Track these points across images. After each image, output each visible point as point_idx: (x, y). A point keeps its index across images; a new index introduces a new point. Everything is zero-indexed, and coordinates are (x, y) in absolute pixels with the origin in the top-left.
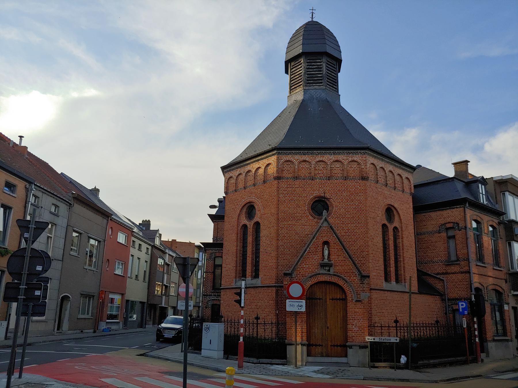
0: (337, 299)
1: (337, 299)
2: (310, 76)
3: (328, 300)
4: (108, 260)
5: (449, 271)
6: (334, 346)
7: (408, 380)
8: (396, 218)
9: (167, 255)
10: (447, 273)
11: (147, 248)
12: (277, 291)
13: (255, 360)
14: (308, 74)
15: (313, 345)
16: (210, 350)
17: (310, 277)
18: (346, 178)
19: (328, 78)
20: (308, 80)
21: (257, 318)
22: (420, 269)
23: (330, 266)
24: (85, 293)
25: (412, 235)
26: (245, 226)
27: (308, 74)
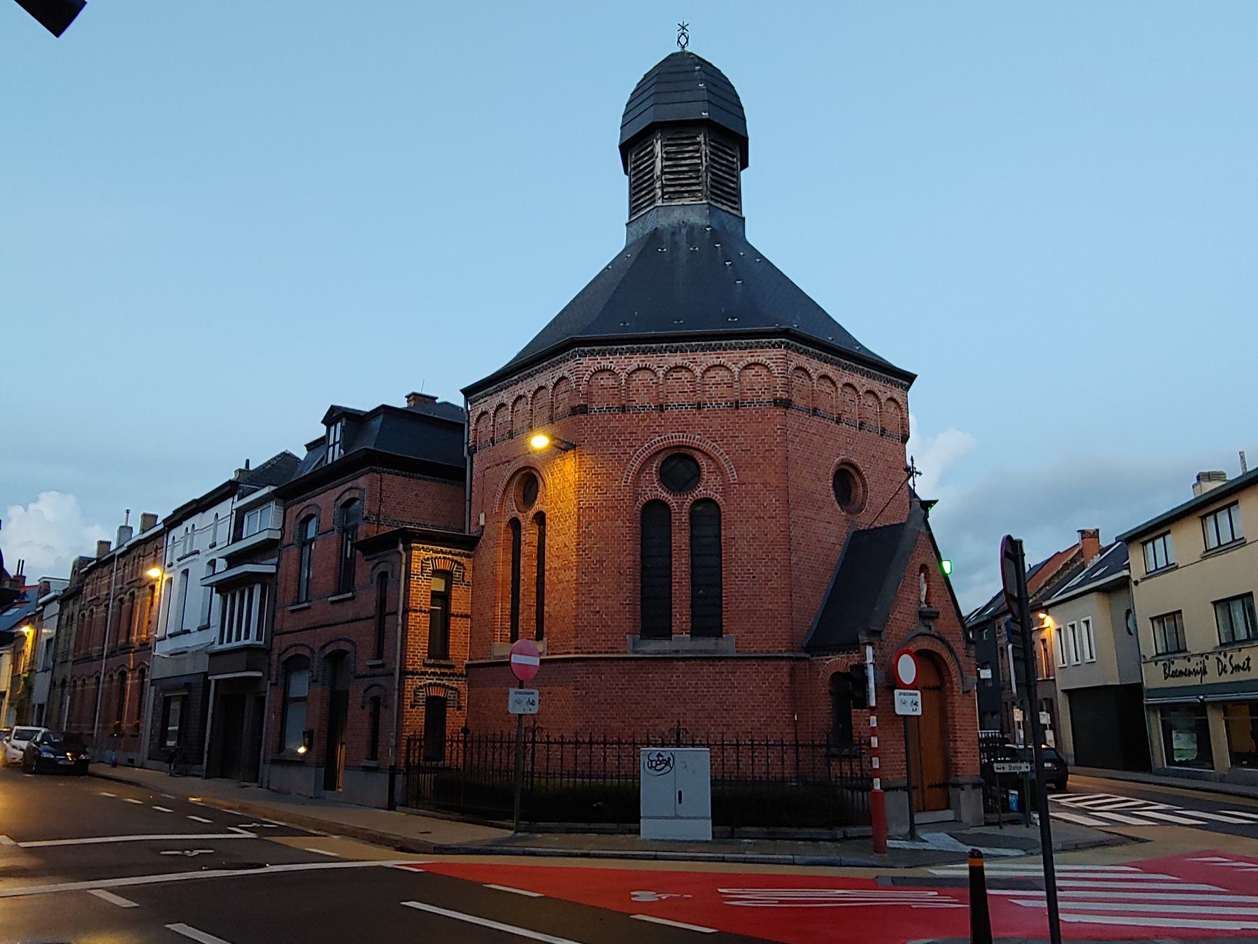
12: (792, 668)
16: (677, 817)
23: (934, 616)
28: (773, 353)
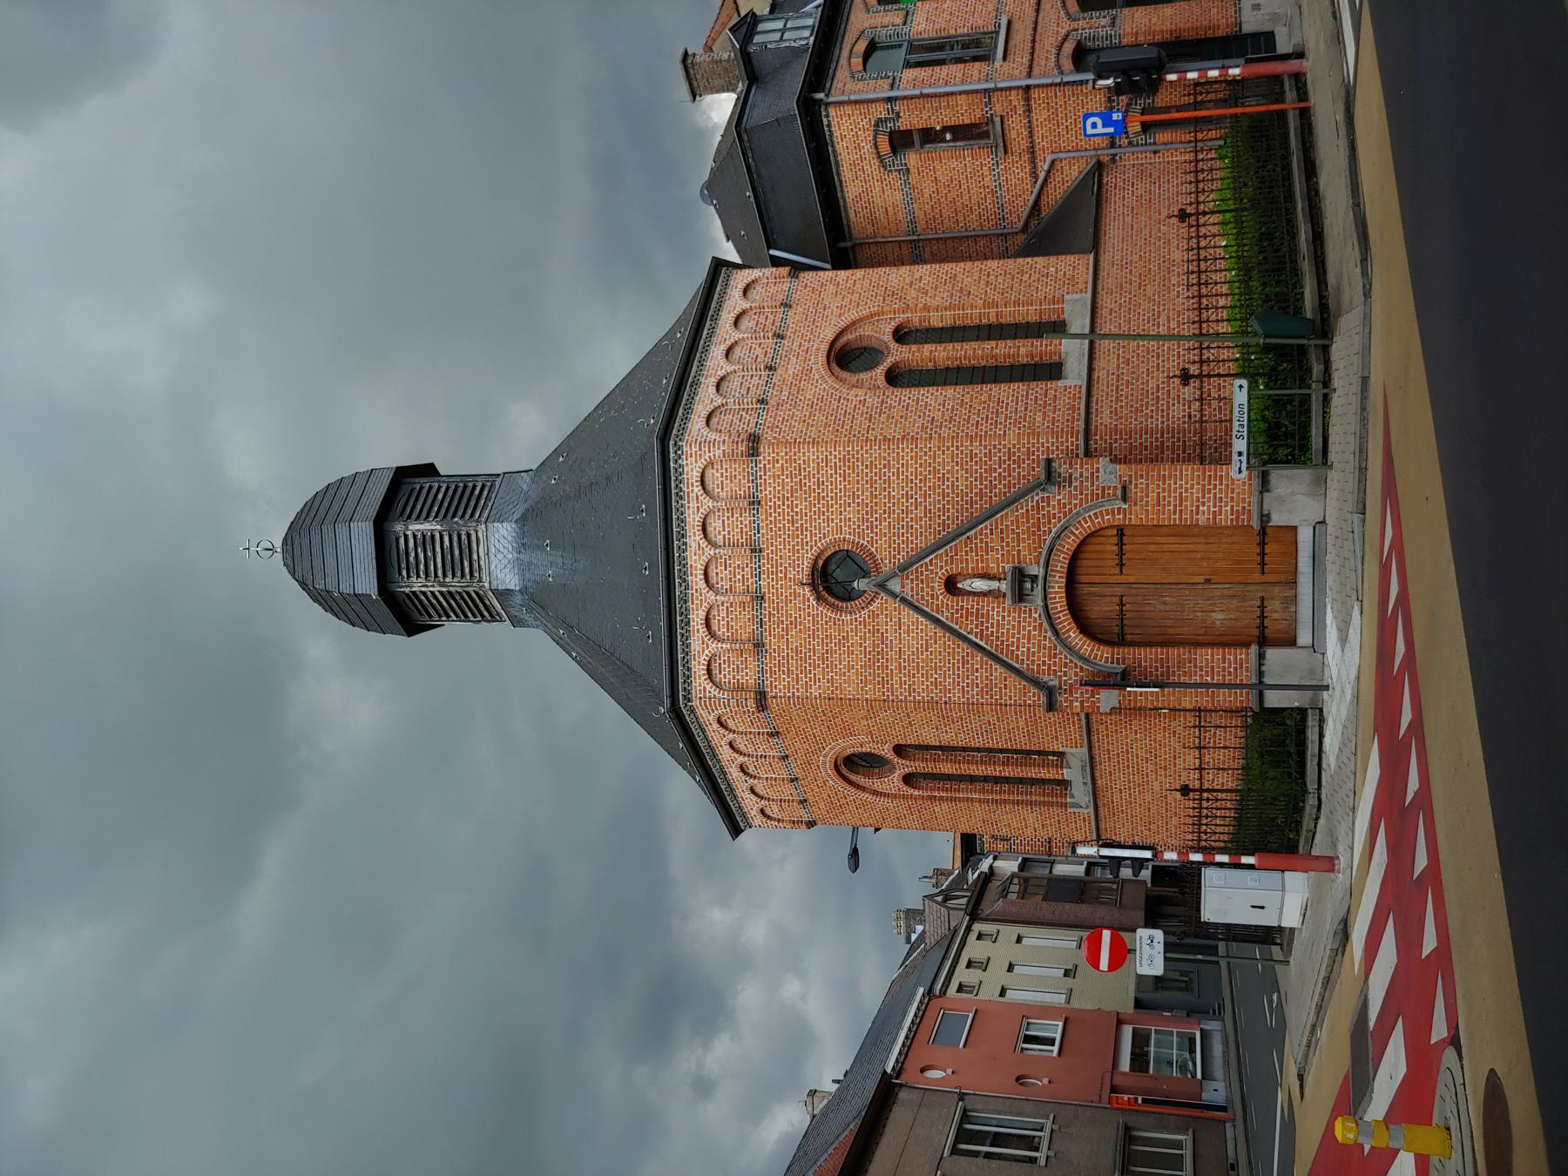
0: (1121, 553)
1: (1121, 553)
2: (449, 567)
3: (1122, 579)
4: (1017, 1080)
5: (1025, 144)
6: (1263, 564)
7: (1365, 381)
8: (866, 331)
9: (998, 864)
10: (1032, 151)
11: (980, 937)
13: (1311, 801)
14: (445, 576)
15: (1262, 627)
17: (1056, 633)
18: (755, 503)
19: (454, 516)
20: (463, 575)
21: (1185, 790)
22: (1020, 225)
23: (1020, 576)
24: (1119, 1160)
25: (917, 275)
26: (908, 779)
27: (445, 576)
28: (702, 712)
